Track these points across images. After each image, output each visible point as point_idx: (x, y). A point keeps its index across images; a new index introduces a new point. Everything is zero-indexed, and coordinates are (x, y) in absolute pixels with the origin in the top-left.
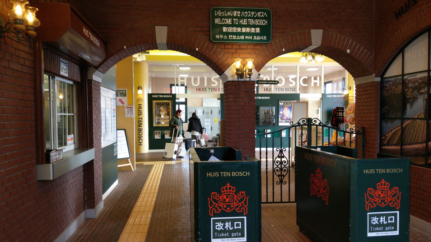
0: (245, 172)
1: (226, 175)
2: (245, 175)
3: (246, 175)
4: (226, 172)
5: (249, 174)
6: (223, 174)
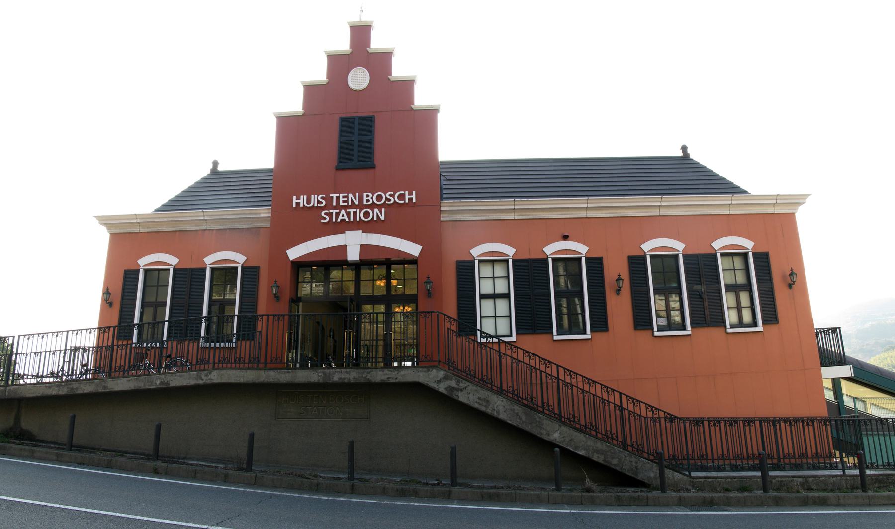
0: (403, 192)
1: (347, 202)
2: (403, 202)
3: (407, 201)
4: (346, 195)
5: (414, 197)
6: (338, 198)
